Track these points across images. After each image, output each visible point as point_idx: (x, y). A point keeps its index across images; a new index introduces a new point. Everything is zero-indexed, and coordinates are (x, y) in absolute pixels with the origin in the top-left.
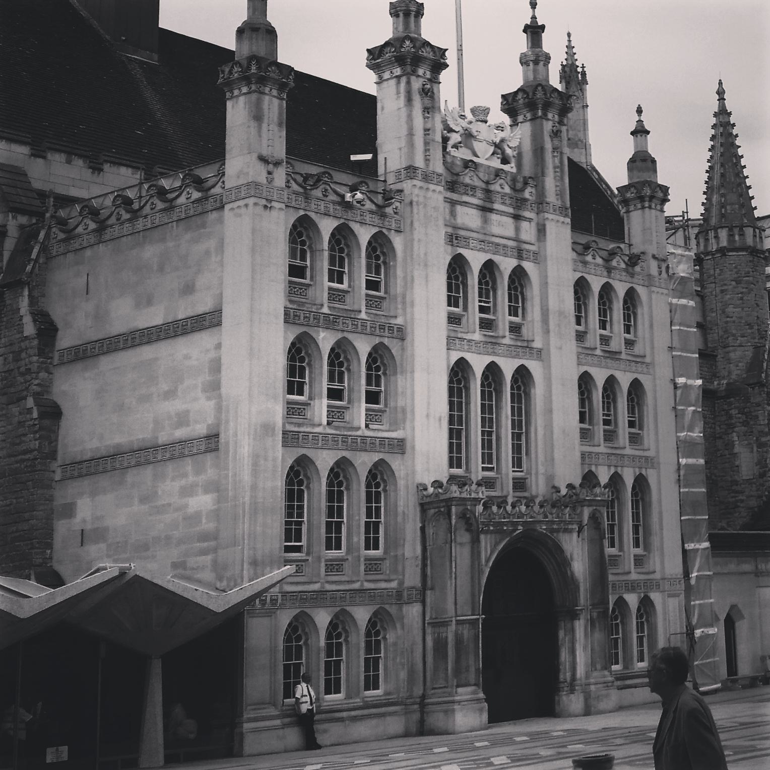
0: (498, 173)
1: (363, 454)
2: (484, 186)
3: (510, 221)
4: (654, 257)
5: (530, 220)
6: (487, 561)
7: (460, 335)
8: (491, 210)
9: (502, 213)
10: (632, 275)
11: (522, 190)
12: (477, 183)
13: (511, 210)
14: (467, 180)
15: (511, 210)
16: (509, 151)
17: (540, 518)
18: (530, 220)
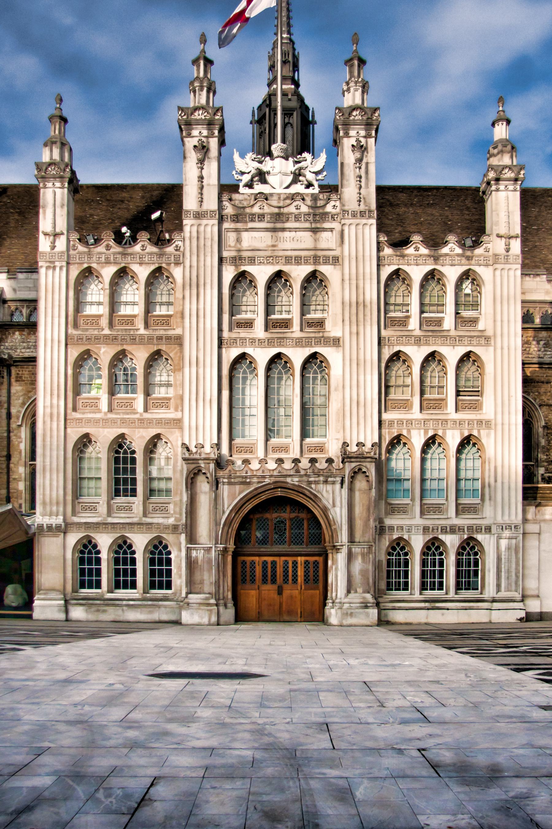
0: (293, 197)
1: (141, 430)
2: (276, 210)
3: (308, 234)
4: (498, 236)
5: (331, 230)
6: (229, 506)
7: (242, 335)
8: (283, 230)
9: (296, 230)
10: (469, 258)
11: (325, 206)
12: (267, 210)
13: (307, 225)
14: (256, 210)
15: (307, 225)
16: (311, 177)
17: (292, 473)
18: (331, 230)
